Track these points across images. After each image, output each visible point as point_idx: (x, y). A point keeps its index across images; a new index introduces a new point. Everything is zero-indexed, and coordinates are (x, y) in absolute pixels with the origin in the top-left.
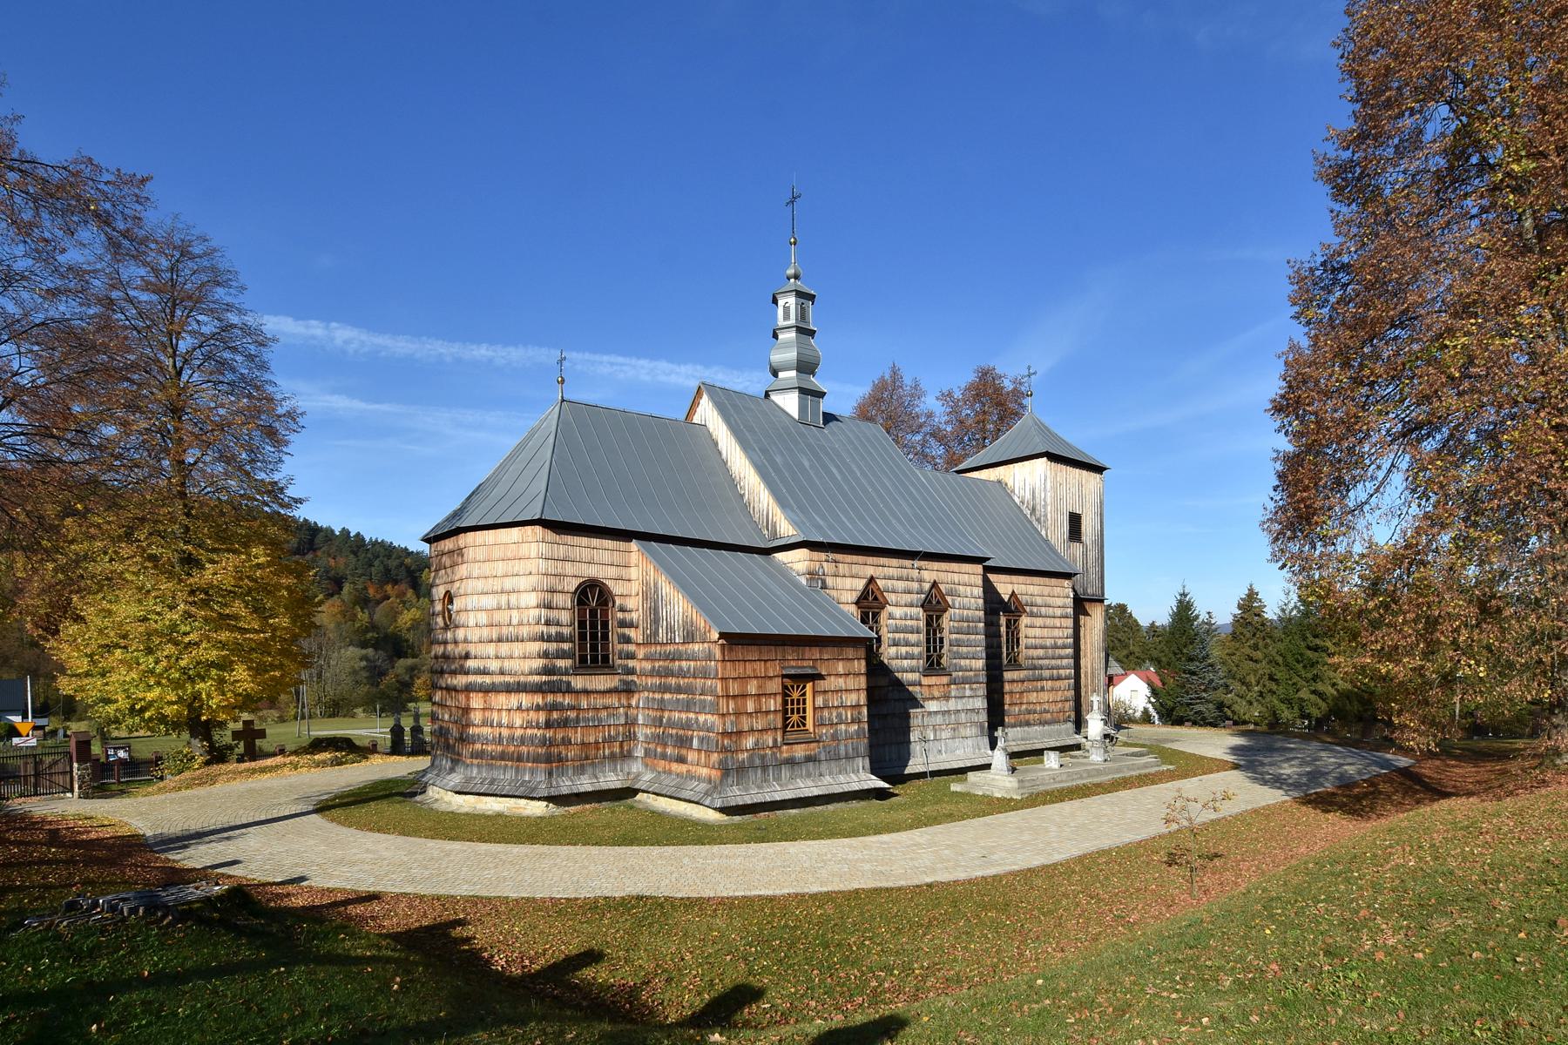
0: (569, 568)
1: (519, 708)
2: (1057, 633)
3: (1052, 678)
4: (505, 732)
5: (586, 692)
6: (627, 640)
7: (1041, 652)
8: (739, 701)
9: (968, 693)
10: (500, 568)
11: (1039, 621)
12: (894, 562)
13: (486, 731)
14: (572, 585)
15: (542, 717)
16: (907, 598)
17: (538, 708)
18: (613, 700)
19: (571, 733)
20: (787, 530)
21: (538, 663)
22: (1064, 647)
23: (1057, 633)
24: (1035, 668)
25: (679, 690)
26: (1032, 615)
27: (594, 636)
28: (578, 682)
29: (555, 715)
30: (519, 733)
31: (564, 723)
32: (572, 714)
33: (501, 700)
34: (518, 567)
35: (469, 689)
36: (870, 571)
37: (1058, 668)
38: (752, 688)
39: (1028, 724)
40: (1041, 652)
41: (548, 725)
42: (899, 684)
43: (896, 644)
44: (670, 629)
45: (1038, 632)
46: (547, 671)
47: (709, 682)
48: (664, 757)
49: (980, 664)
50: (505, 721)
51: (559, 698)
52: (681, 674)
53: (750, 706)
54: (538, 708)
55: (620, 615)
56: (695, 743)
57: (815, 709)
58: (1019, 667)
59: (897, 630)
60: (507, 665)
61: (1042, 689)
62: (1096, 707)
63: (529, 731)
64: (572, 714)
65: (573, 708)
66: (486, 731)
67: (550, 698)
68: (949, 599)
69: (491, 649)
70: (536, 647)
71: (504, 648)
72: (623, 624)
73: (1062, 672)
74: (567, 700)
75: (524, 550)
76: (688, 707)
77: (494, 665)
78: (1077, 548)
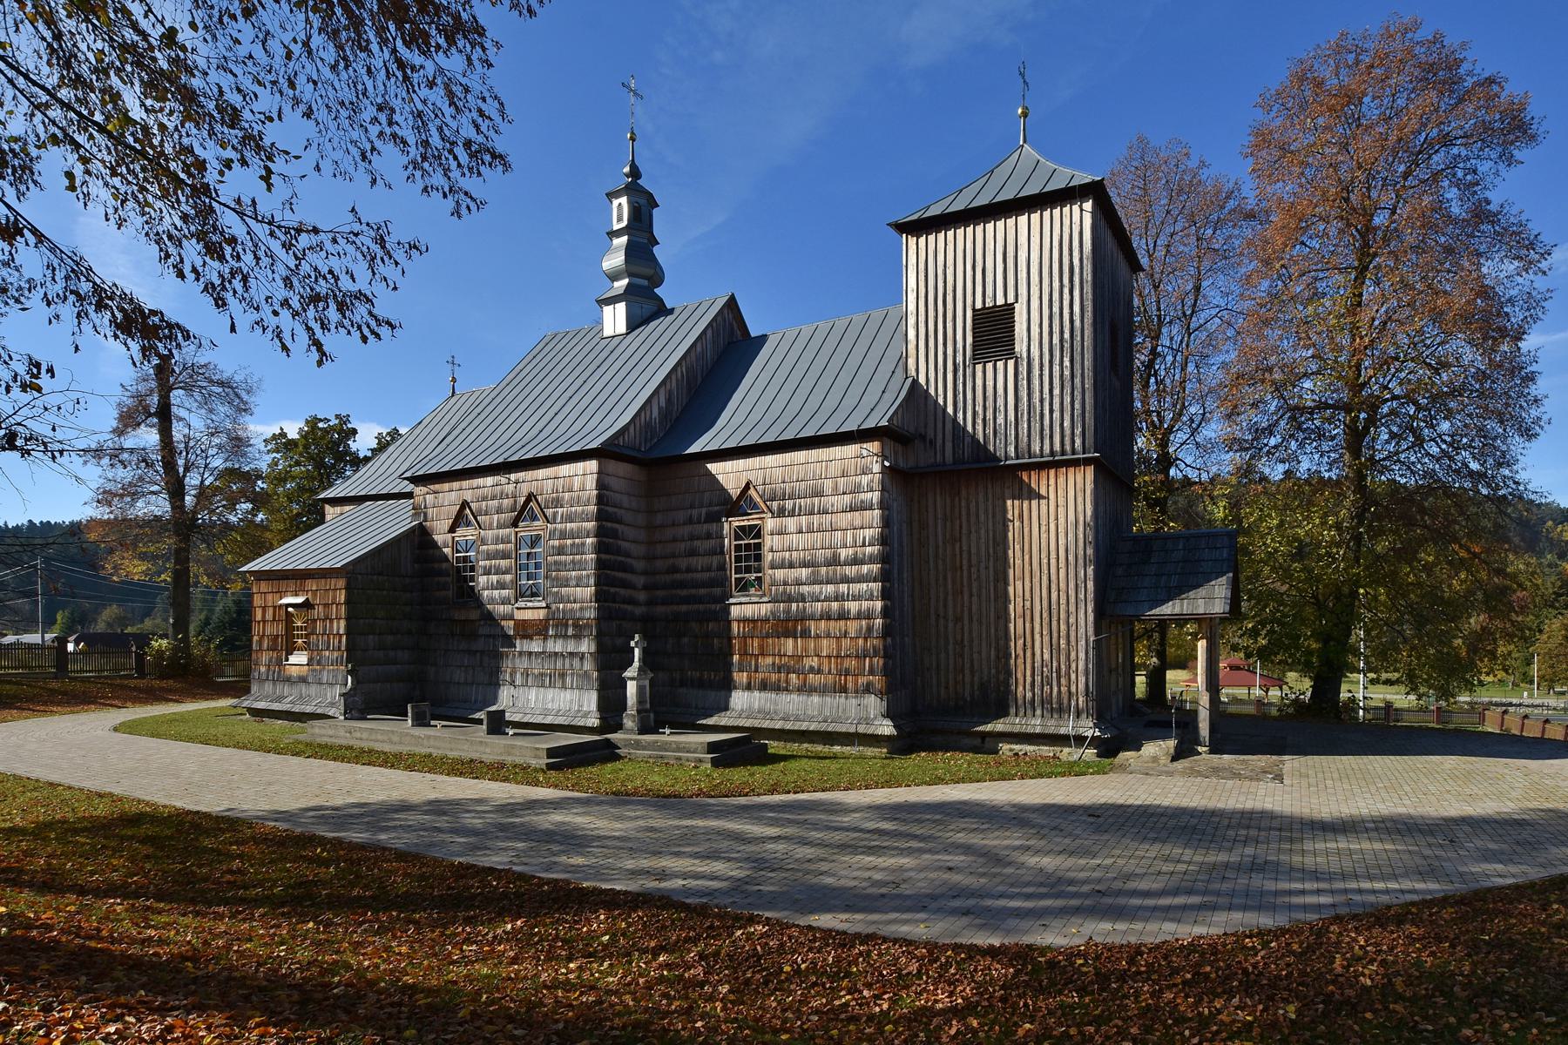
3: (827, 616)
9: (570, 632)
11: (791, 523)
12: (490, 481)
22: (855, 561)
24: (789, 599)
26: (781, 513)
37: (827, 599)
39: (777, 688)
40: (804, 573)
42: (489, 617)
43: (487, 572)
49: (589, 591)
59: (489, 556)
61: (805, 634)
68: (549, 512)
73: (853, 607)
78: (998, 376)
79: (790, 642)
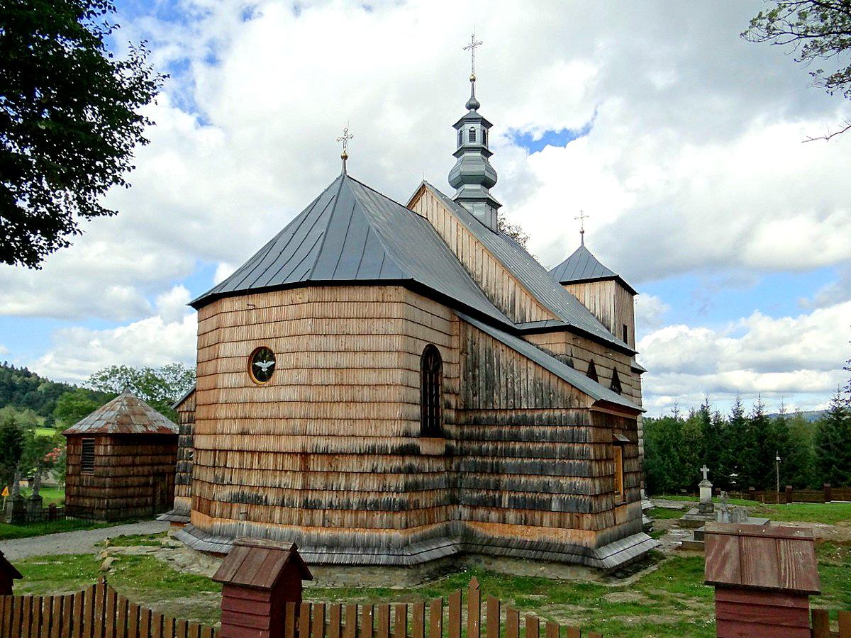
1: (373, 471)
4: (354, 499)
6: (448, 406)
10: (354, 326)
13: (326, 498)
17: (398, 471)
18: (441, 465)
20: (536, 317)
25: (530, 454)
28: (425, 446)
29: (411, 479)
30: (372, 497)
33: (353, 464)
34: (379, 326)
35: (305, 455)
36: (590, 357)
44: (511, 394)
46: (407, 435)
47: (577, 447)
48: (504, 521)
50: (355, 483)
52: (531, 438)
54: (398, 471)
56: (555, 506)
60: (359, 428)
62: (705, 476)
63: (385, 497)
66: (326, 498)
69: (339, 411)
71: (356, 411)
74: (416, 462)
75: (384, 309)
76: (543, 471)
77: (342, 428)
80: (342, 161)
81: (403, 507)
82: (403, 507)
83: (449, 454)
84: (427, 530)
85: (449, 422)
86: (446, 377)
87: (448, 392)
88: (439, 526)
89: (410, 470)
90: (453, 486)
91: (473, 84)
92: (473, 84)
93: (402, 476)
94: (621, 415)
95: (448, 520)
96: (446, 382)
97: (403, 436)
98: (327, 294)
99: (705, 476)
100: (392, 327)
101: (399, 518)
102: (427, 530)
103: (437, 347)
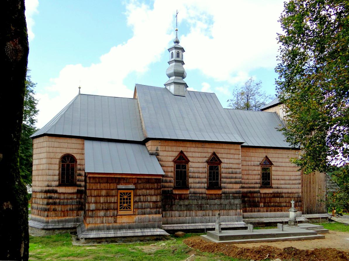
0: (58, 150)
2: (291, 173)
5: (64, 193)
6: (80, 175)
7: (282, 182)
8: (98, 198)
11: (278, 168)
14: (60, 156)
15: (45, 201)
16: (201, 160)
18: (75, 196)
19: (57, 207)
21: (46, 183)
23: (291, 173)
27: (68, 173)
28: (61, 190)
30: (41, 206)
31: (55, 204)
32: (58, 201)
36: (181, 149)
38: (104, 193)
40: (282, 182)
41: (48, 204)
45: (280, 173)
51: (53, 195)
53: (102, 200)
54: (45, 198)
55: (79, 167)
57: (134, 202)
58: (271, 187)
61: (282, 197)
64: (58, 201)
65: (56, 198)
67: (49, 195)
70: (45, 178)
72: (80, 170)
74: (56, 195)
79: (278, 199)
80: (79, 89)
81: (45, 210)
82: (45, 210)
83: (79, 192)
84: (64, 218)
85: (81, 181)
86: (79, 165)
87: (80, 170)
88: (72, 217)
89: (50, 198)
90: (79, 203)
91: (177, 32)
92: (177, 32)
93: (46, 200)
94: (134, 177)
95: (79, 216)
96: (79, 167)
97: (46, 186)
98: (53, 139)
99: (293, 205)
100: (44, 150)
101: (46, 213)
102: (64, 218)
103: (72, 154)
